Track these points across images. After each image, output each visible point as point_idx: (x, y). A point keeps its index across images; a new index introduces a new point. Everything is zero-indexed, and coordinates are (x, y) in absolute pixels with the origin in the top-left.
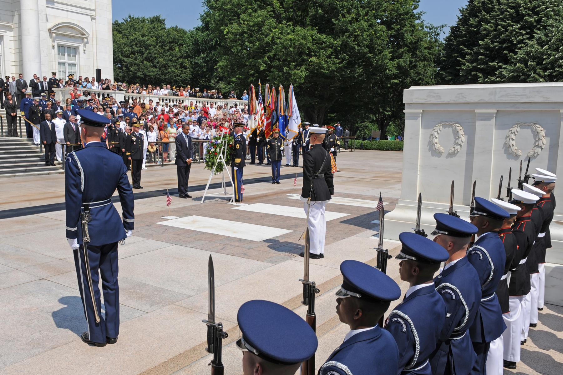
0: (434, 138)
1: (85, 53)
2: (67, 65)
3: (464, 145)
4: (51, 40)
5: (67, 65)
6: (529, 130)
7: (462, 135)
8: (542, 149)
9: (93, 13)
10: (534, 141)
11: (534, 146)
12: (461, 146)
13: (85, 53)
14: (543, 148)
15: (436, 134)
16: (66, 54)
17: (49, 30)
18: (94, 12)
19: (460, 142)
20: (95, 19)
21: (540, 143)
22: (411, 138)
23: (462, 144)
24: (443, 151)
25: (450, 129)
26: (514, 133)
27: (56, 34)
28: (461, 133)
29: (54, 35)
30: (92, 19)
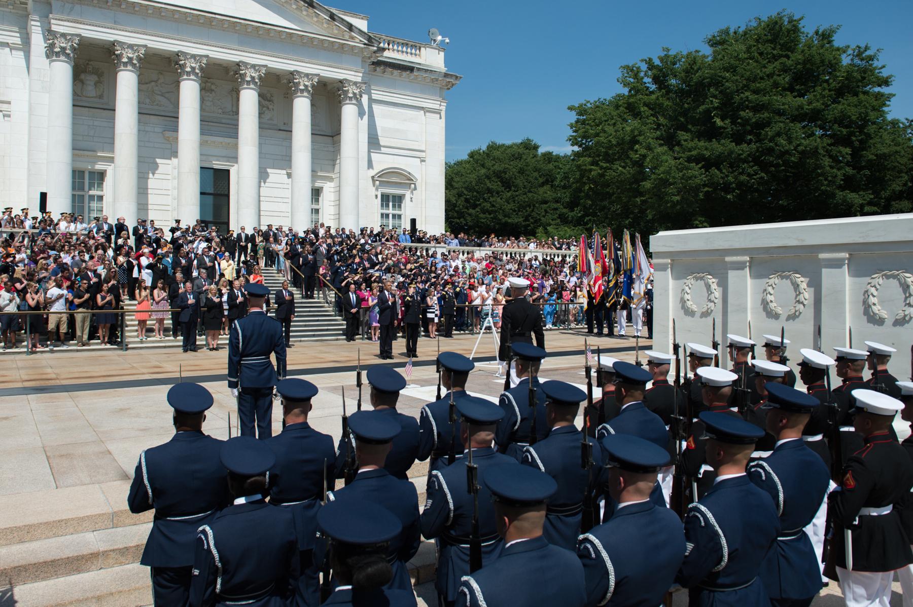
0: (686, 294)
1: (412, 201)
2: (391, 216)
3: (719, 302)
4: (374, 188)
5: (391, 216)
6: (788, 281)
7: (715, 290)
8: (804, 305)
10: (794, 294)
11: (795, 301)
12: (715, 303)
13: (412, 201)
14: (805, 303)
15: (687, 288)
16: (391, 204)
17: (373, 177)
18: (424, 154)
19: (713, 299)
20: (424, 161)
21: (801, 298)
23: (716, 301)
24: (696, 310)
25: (702, 282)
26: (772, 285)
27: (380, 181)
28: (714, 286)
29: (377, 183)
30: (422, 161)
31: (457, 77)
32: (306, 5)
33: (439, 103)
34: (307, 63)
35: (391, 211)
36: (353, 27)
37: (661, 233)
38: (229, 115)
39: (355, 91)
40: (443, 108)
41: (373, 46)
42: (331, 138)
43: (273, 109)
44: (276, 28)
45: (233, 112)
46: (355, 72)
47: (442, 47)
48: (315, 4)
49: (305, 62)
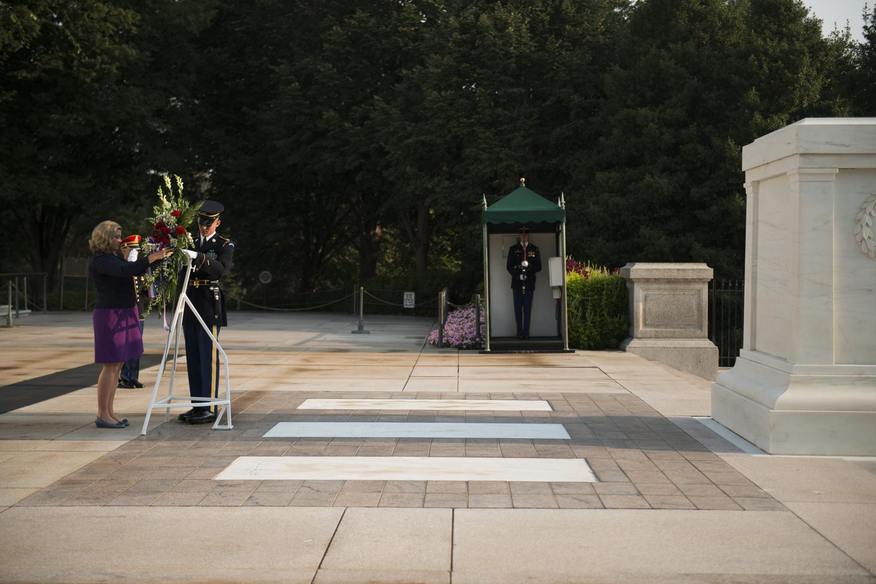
22: (814, 229)
37: (808, 122)
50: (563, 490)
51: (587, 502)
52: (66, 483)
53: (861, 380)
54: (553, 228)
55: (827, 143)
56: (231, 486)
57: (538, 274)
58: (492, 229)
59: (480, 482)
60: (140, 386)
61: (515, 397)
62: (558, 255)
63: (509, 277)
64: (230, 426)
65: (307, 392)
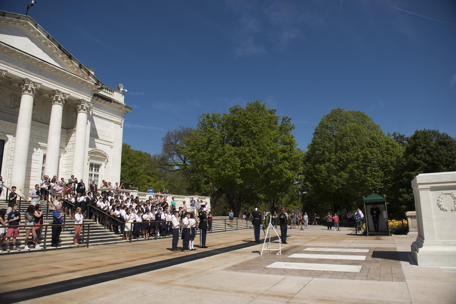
1: (105, 168)
2: (93, 175)
5: (93, 175)
9: (112, 144)
16: (94, 168)
31: (131, 109)
32: (68, 57)
33: (121, 120)
34: (63, 87)
35: (93, 172)
36: (90, 74)
37: (420, 175)
38: (8, 108)
39: (87, 106)
40: (123, 122)
41: (99, 85)
42: (66, 130)
43: (35, 109)
44: (50, 65)
45: (11, 107)
46: (88, 96)
47: (123, 93)
48: (72, 58)
49: (62, 86)
50: (348, 274)
51: (350, 278)
52: (234, 266)
53: (444, 244)
54: (384, 203)
55: (425, 180)
56: (267, 269)
57: (380, 215)
58: (367, 204)
59: (327, 271)
60: (286, 243)
61: (362, 248)
62: (385, 210)
63: (372, 216)
64: (281, 254)
65: (310, 246)
